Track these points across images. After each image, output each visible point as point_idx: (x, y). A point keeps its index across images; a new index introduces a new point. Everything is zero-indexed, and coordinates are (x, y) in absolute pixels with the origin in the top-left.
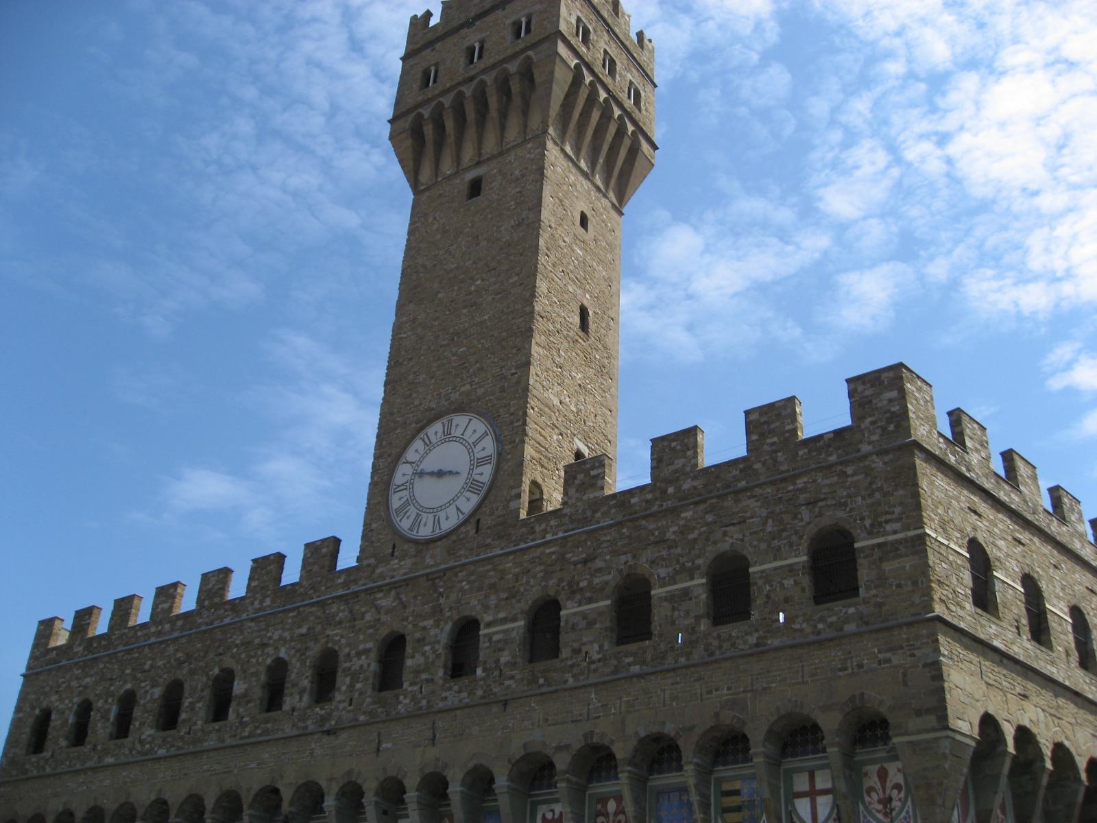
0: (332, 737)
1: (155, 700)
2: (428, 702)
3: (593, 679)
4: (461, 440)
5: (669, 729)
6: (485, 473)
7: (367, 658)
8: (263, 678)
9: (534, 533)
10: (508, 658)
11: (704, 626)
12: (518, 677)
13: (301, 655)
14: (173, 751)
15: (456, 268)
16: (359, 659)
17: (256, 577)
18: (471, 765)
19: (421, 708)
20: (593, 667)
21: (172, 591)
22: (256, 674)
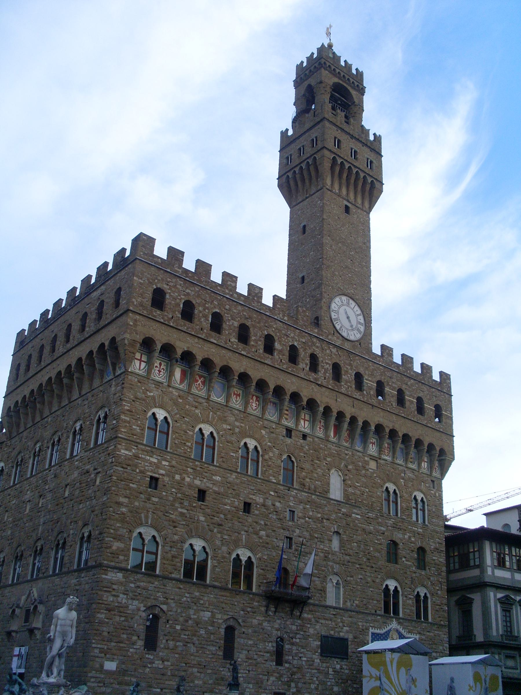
0: (320, 388)
1: (235, 327)
4: (353, 309)
5: (410, 434)
6: (362, 329)
8: (289, 349)
11: (416, 412)
14: (249, 355)
18: (364, 419)
22: (285, 345)
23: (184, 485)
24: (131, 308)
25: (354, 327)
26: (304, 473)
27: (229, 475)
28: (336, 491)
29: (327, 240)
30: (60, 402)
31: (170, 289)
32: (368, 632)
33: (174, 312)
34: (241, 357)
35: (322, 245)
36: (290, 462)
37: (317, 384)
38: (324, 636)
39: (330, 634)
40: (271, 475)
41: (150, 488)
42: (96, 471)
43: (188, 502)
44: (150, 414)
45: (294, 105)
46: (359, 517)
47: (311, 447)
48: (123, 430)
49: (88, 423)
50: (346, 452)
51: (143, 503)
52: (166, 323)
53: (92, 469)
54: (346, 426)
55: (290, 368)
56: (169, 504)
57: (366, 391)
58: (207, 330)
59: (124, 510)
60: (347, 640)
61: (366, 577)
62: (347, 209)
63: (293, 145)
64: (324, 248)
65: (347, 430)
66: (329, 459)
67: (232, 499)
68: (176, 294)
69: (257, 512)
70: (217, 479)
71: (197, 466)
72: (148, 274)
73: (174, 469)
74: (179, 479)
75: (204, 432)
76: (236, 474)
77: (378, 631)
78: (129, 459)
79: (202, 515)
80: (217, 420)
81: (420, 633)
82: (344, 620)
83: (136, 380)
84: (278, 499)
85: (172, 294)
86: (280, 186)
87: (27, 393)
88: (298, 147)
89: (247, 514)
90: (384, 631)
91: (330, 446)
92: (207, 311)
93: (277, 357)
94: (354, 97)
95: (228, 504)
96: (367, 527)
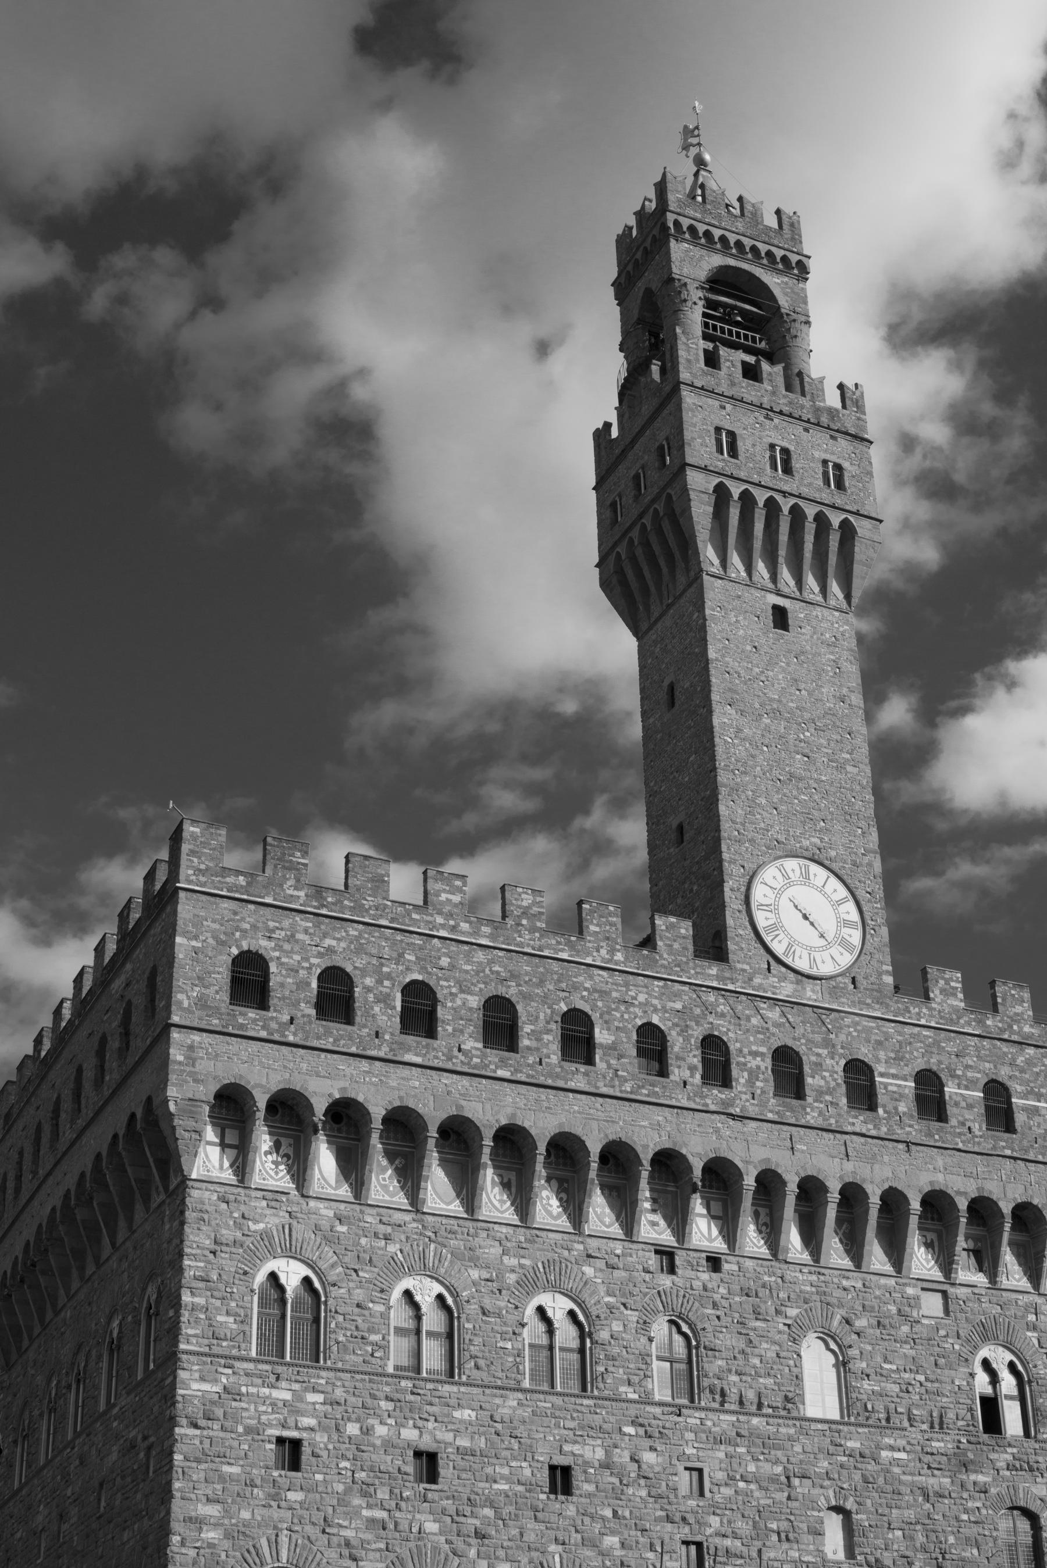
0: (739, 1123)
1: (471, 1009)
2: (837, 1122)
3: (976, 1149)
4: (821, 890)
7: (763, 1060)
8: (635, 1037)
9: (909, 1012)
10: (905, 1110)
12: (916, 1127)
13: (682, 1031)
15: (780, 701)
16: (754, 1059)
17: (595, 922)
18: (886, 1186)
19: (831, 1125)
20: (976, 1140)
21: (458, 883)
23: (374, 1446)
24: (175, 1019)
25: (830, 936)
26: (720, 1362)
27: (498, 1401)
28: (821, 1398)
29: (723, 717)
30: (82, 1269)
31: (278, 947)
33: (296, 1004)
34: (497, 1085)
35: (710, 730)
36: (678, 1339)
37: (733, 1117)
40: (619, 1382)
41: (277, 1468)
42: (147, 1443)
43: (387, 1489)
44: (261, 1277)
45: (621, 350)
46: (903, 1455)
47: (736, 1288)
48: (190, 1331)
49: (130, 1318)
50: (845, 1283)
51: (265, 1511)
52: (276, 1037)
53: (140, 1437)
54: (831, 1212)
55: (643, 1087)
56: (335, 1502)
57: (884, 1106)
58: (392, 1034)
59: (211, 1535)
62: (781, 618)
63: (621, 469)
64: (717, 740)
65: (839, 1221)
66: (792, 1312)
67: (514, 1464)
68: (297, 958)
69: (589, 1488)
70: (466, 1417)
71: (403, 1391)
72: (214, 921)
73: (341, 1409)
74: (357, 1432)
75: (418, 1298)
76: (520, 1395)
78: (213, 1403)
79: (431, 1517)
80: (451, 1262)
83: (215, 1197)
84: (648, 1443)
85: (284, 960)
86: (605, 585)
87: (18, 1250)
88: (633, 473)
89: (561, 1497)
91: (791, 1274)
92: (387, 983)
93: (604, 1065)
94: (777, 292)
95: (503, 1477)
96: (932, 1481)
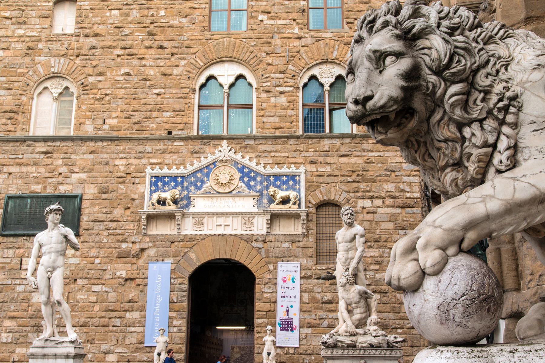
32: (145, 177)
38: (10, 198)
39: (31, 192)
60: (76, 197)
61: (143, 69)
77: (174, 171)
81: (312, 163)
82: (76, 160)
90: (190, 169)
